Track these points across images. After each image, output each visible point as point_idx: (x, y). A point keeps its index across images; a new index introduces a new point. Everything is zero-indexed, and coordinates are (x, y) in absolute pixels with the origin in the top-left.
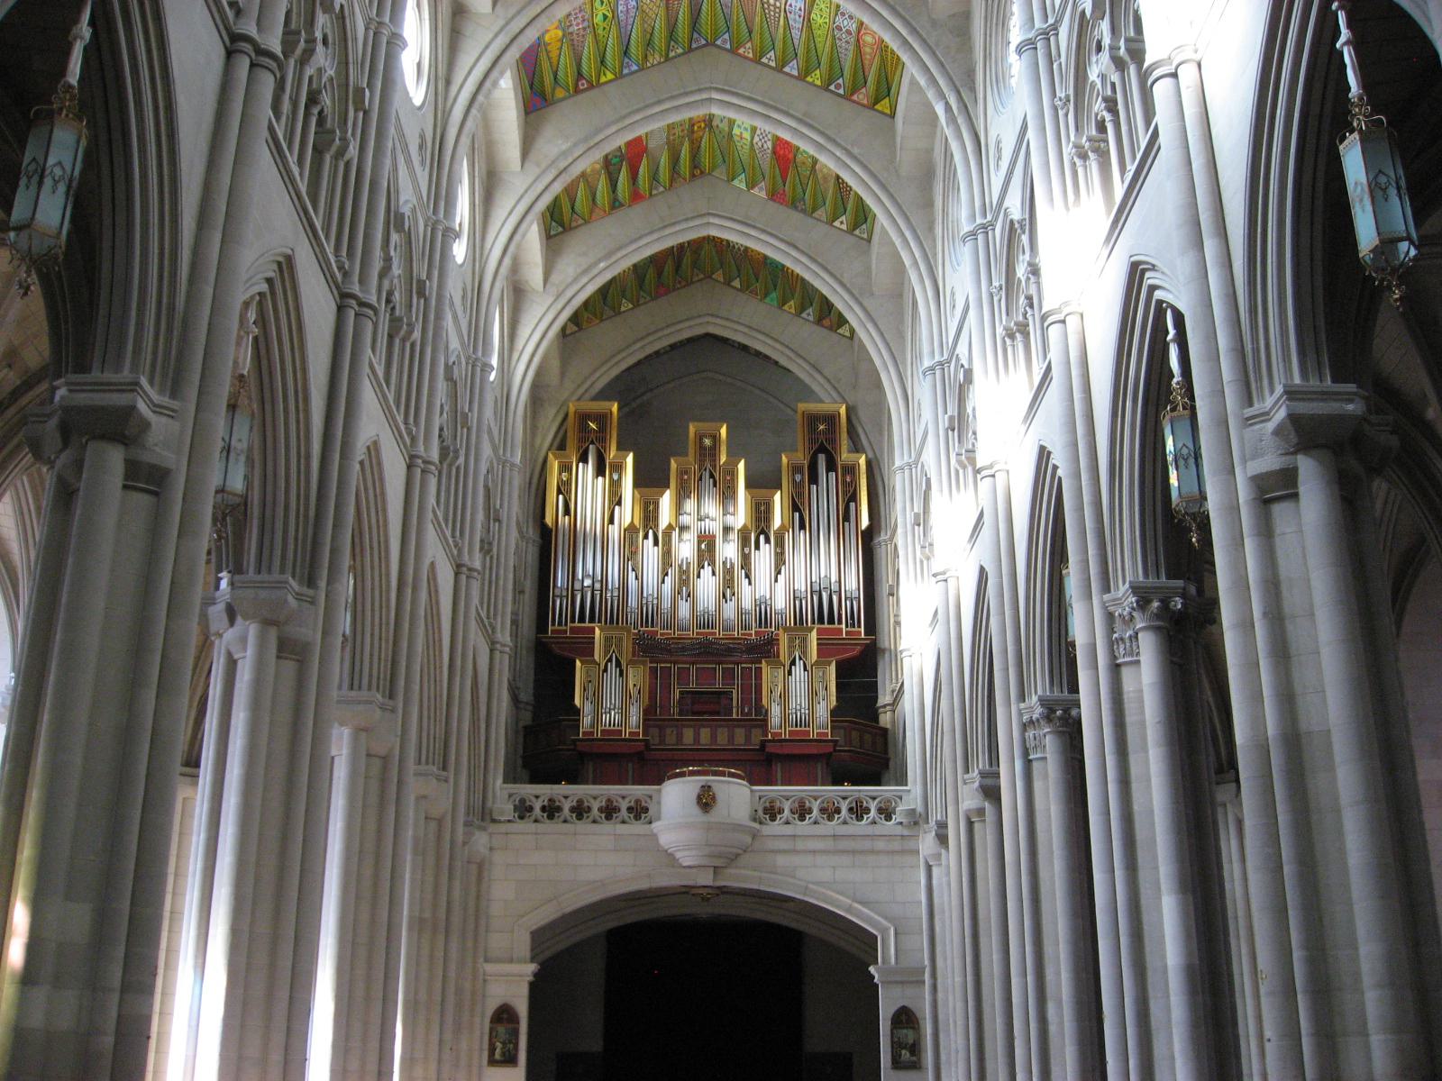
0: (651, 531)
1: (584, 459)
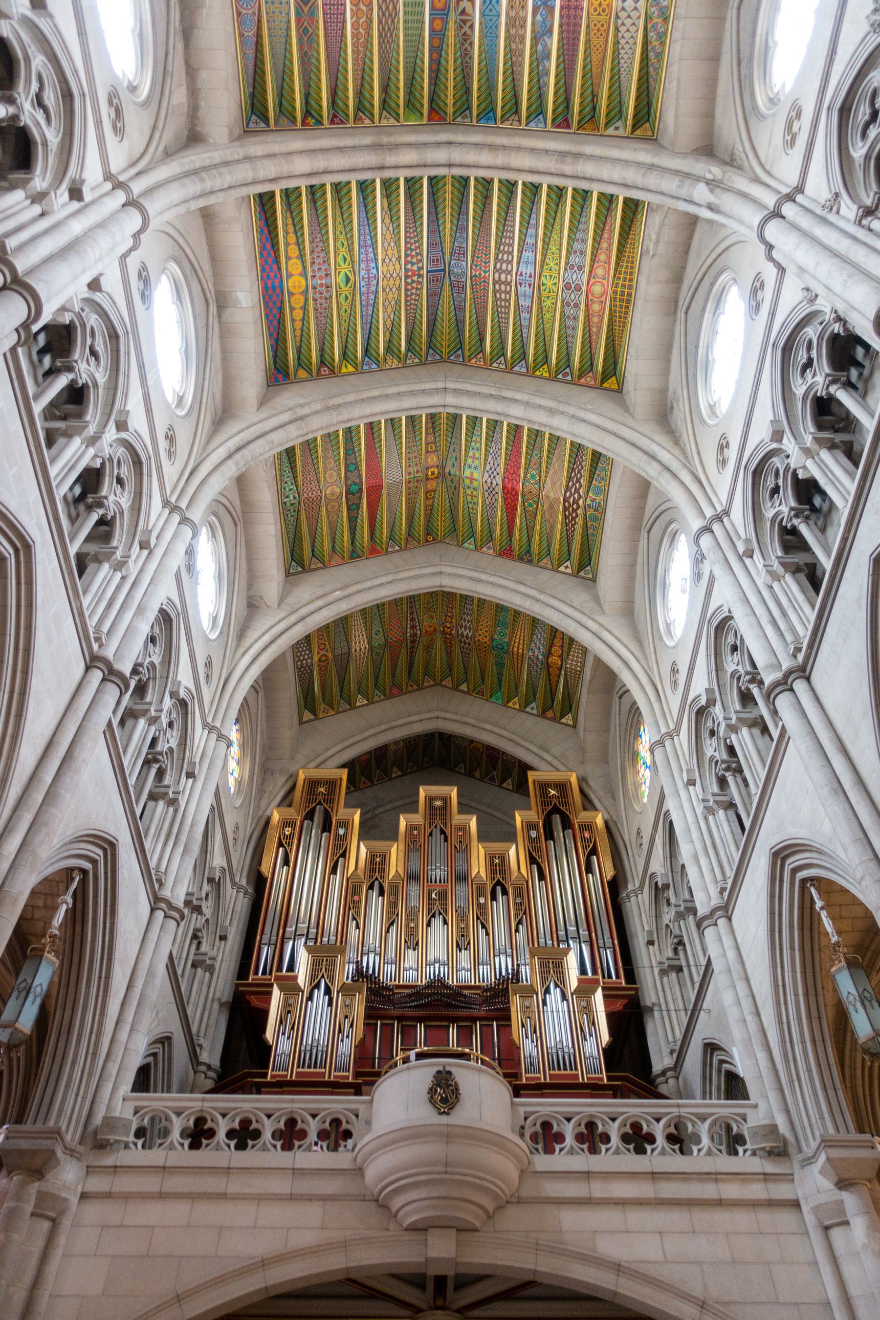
0: (376, 883)
1: (310, 816)
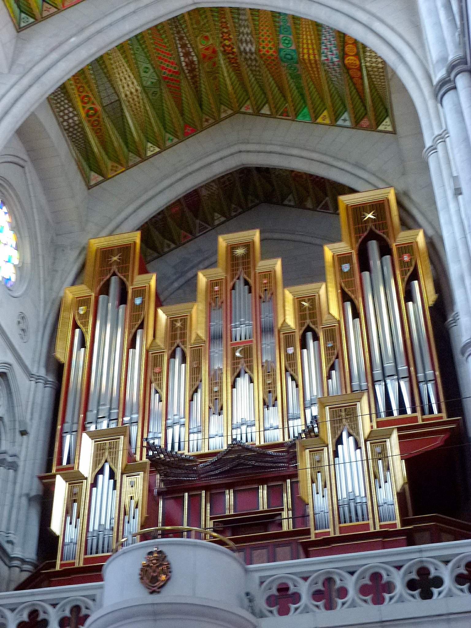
1: (105, 290)
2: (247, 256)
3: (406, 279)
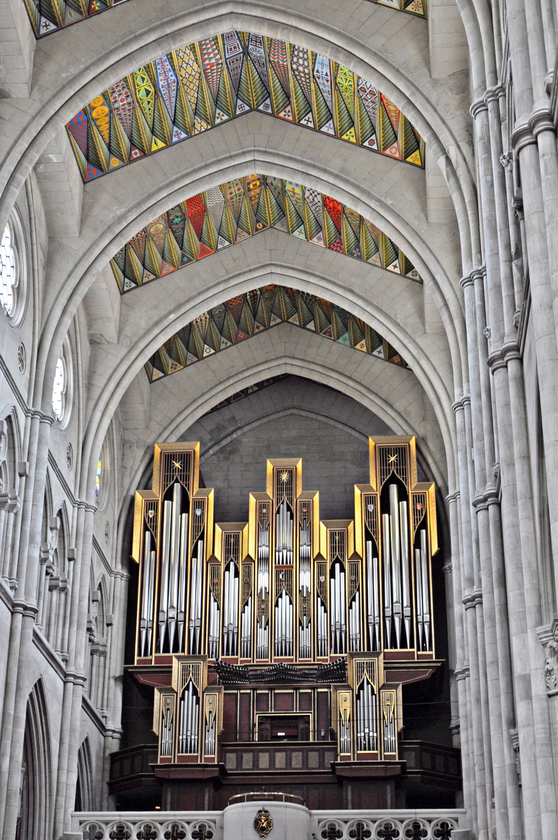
0: (232, 564)
1: (169, 496)
2: (291, 481)
3: (417, 527)
